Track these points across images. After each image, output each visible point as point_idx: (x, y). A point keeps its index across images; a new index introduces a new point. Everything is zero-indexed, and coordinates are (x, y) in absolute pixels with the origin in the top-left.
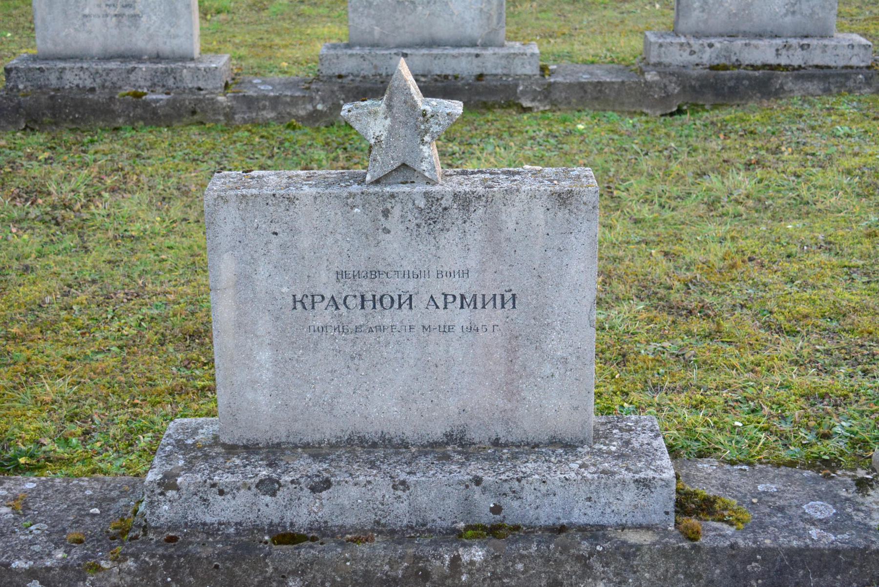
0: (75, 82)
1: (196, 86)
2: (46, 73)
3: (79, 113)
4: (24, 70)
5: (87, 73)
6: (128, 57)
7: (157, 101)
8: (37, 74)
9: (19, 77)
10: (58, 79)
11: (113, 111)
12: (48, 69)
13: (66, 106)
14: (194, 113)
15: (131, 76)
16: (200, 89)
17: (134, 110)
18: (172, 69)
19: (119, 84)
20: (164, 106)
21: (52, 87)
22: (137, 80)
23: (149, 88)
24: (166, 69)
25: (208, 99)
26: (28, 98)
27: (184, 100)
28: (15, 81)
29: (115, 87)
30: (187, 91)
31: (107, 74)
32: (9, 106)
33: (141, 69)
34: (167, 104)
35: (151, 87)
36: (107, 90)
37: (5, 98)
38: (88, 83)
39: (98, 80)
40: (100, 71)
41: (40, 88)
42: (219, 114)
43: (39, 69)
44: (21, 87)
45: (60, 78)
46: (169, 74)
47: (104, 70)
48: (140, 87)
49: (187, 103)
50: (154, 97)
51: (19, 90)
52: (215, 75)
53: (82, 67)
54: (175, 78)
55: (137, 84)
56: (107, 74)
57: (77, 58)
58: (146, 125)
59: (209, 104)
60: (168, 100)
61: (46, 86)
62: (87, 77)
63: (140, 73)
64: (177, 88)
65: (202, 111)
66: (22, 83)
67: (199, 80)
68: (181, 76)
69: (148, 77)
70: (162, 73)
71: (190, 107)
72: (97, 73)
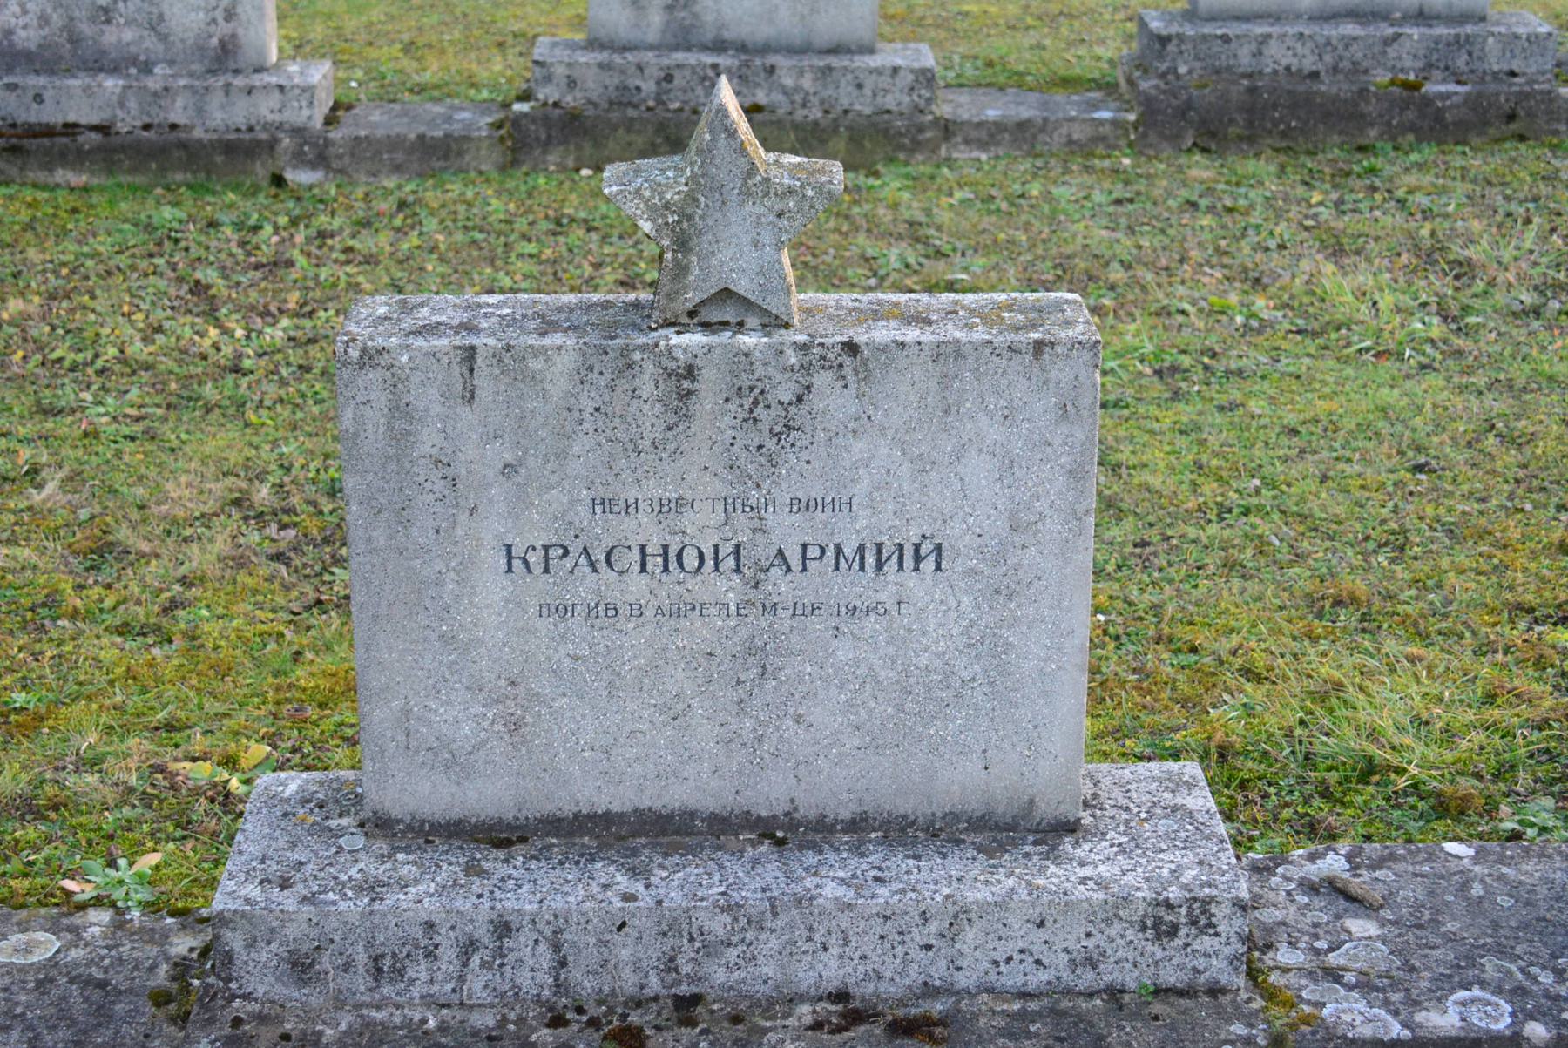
0: (1284, 62)
1: (1506, 67)
2: (1233, 45)
3: (1299, 119)
4: (1193, 39)
5: (1310, 44)
6: (1365, 15)
7: (1448, 96)
8: (1217, 47)
9: (1181, 52)
10: (1254, 55)
11: (1363, 116)
12: (1237, 37)
13: (1275, 106)
14: (1511, 117)
15: (1389, 50)
16: (1513, 74)
17: (1401, 114)
18: (1468, 36)
19: (1365, 64)
20: (1457, 106)
21: (1241, 70)
22: (1400, 58)
23: (1417, 71)
24: (1457, 36)
25: (1542, 92)
26: (1207, 91)
27: (1497, 94)
28: (1174, 60)
29: (1357, 69)
30: (1488, 78)
31: (1347, 47)
32: (1169, 106)
33: (1410, 36)
34: (1466, 102)
35: (1423, 69)
36: (1341, 77)
37: (1164, 92)
38: (1309, 64)
39: (1328, 58)
40: (1334, 42)
41: (1218, 72)
42: (1558, 120)
43: (1221, 37)
44: (1182, 70)
45: (1258, 54)
46: (1461, 47)
47: (1343, 38)
48: (1402, 70)
49: (1502, 99)
50: (1443, 88)
51: (1178, 77)
52: (1545, 48)
53: (1302, 34)
54: (1470, 54)
55: (1399, 66)
56: (1347, 47)
57: (1270, 16)
58: (1419, 140)
59: (1543, 101)
60: (1468, 94)
61: (1229, 69)
62: (1307, 52)
63: (1408, 44)
64: (1472, 71)
65: (1528, 115)
66: (1185, 63)
67: (1513, 57)
68: (1482, 50)
69: (1421, 53)
70: (1448, 44)
71: (1506, 107)
72: (1329, 43)
